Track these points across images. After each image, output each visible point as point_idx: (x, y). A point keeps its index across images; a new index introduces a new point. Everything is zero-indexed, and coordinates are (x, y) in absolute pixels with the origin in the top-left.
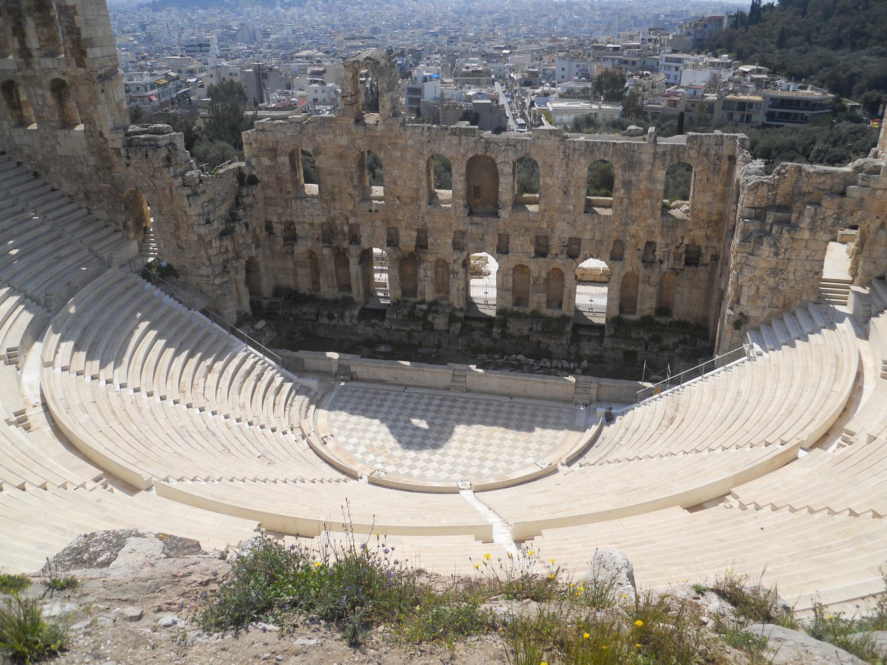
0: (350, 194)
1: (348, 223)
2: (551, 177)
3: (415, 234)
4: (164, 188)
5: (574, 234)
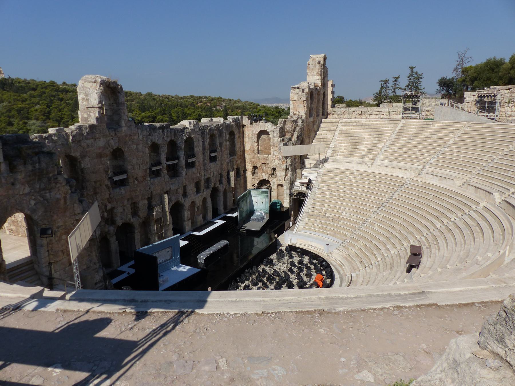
0: (106, 185)
1: (106, 209)
2: (199, 146)
3: (146, 202)
4: (58, 200)
5: (208, 176)
